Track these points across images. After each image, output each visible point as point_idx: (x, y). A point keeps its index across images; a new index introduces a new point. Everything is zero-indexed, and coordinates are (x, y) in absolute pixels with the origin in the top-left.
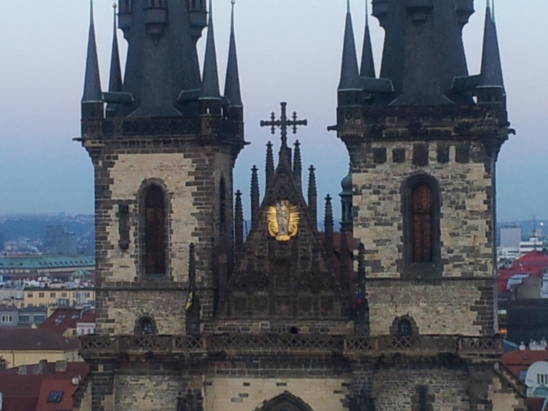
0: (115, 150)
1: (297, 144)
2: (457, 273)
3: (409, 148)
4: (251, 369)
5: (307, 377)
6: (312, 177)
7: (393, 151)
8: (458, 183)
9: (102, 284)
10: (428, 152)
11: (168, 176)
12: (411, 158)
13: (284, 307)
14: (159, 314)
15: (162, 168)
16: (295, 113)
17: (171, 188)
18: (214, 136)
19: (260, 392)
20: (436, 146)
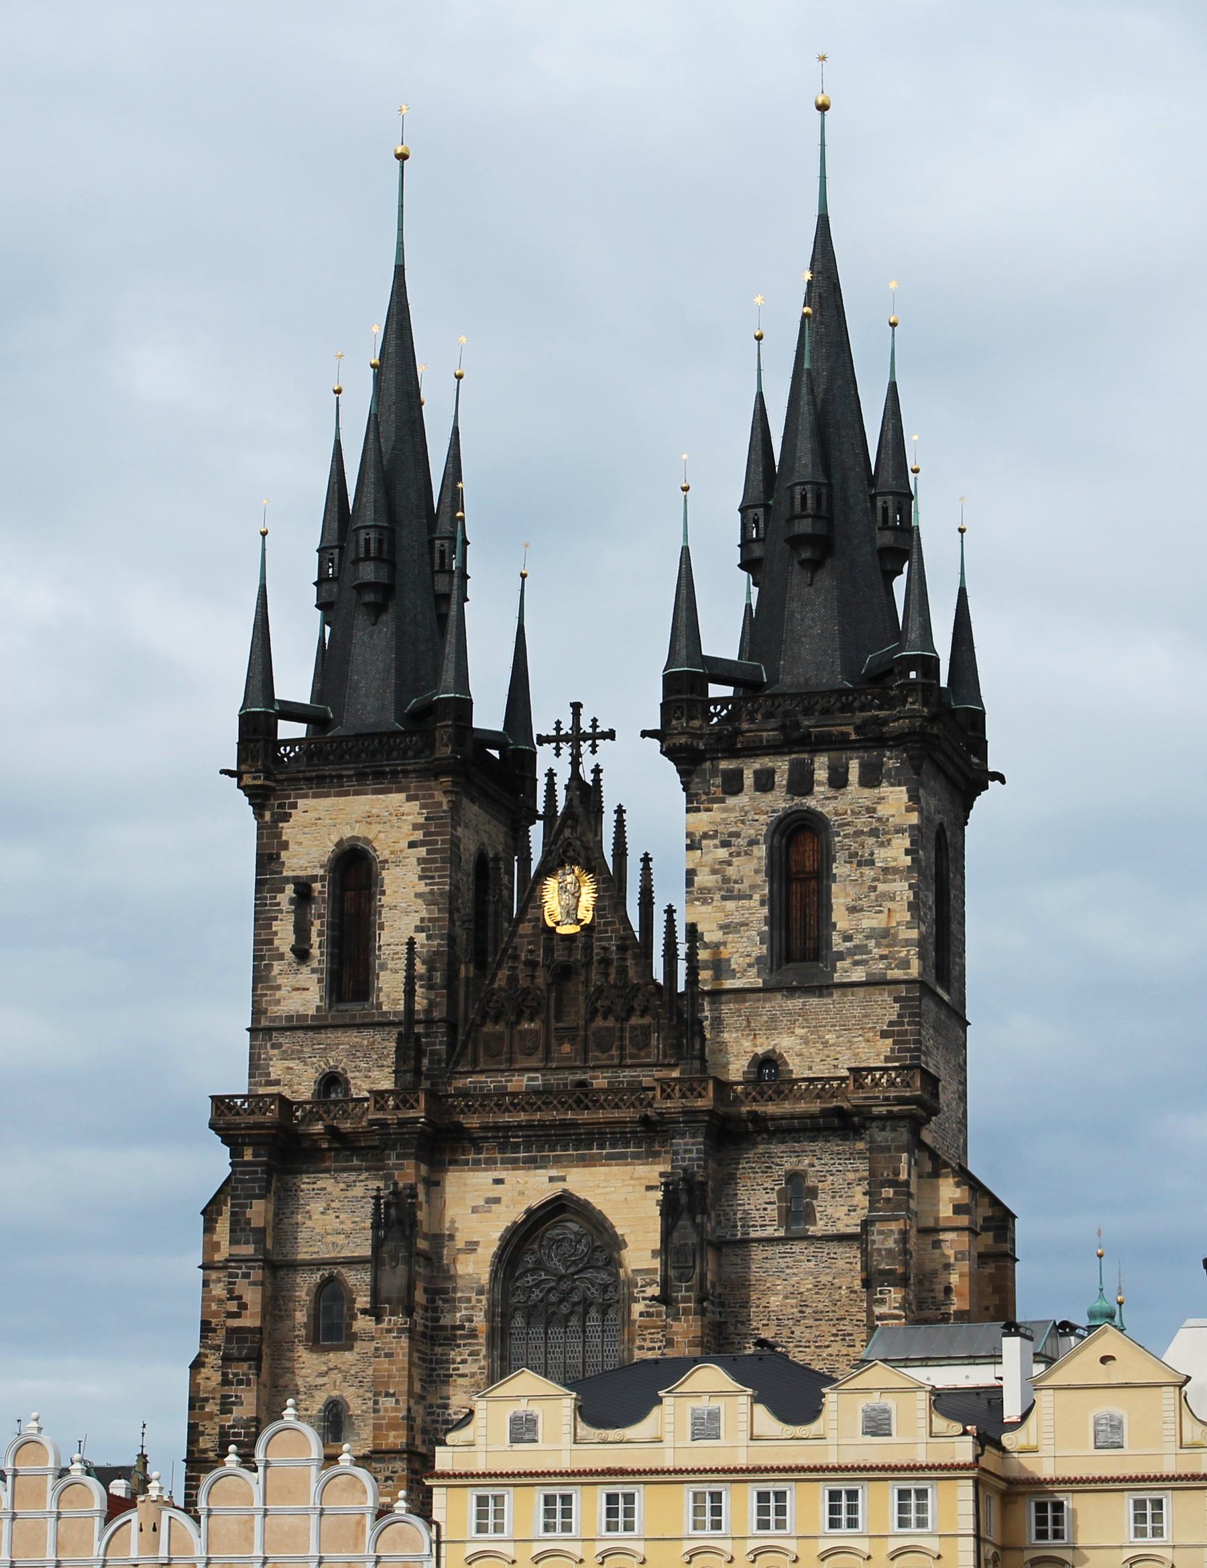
0: (293, 793)
1: (597, 771)
2: (858, 975)
3: (782, 766)
6: (620, 824)
7: (755, 772)
8: (862, 822)
12: (784, 782)
16: (595, 720)
17: (383, 853)
19: (522, 1193)
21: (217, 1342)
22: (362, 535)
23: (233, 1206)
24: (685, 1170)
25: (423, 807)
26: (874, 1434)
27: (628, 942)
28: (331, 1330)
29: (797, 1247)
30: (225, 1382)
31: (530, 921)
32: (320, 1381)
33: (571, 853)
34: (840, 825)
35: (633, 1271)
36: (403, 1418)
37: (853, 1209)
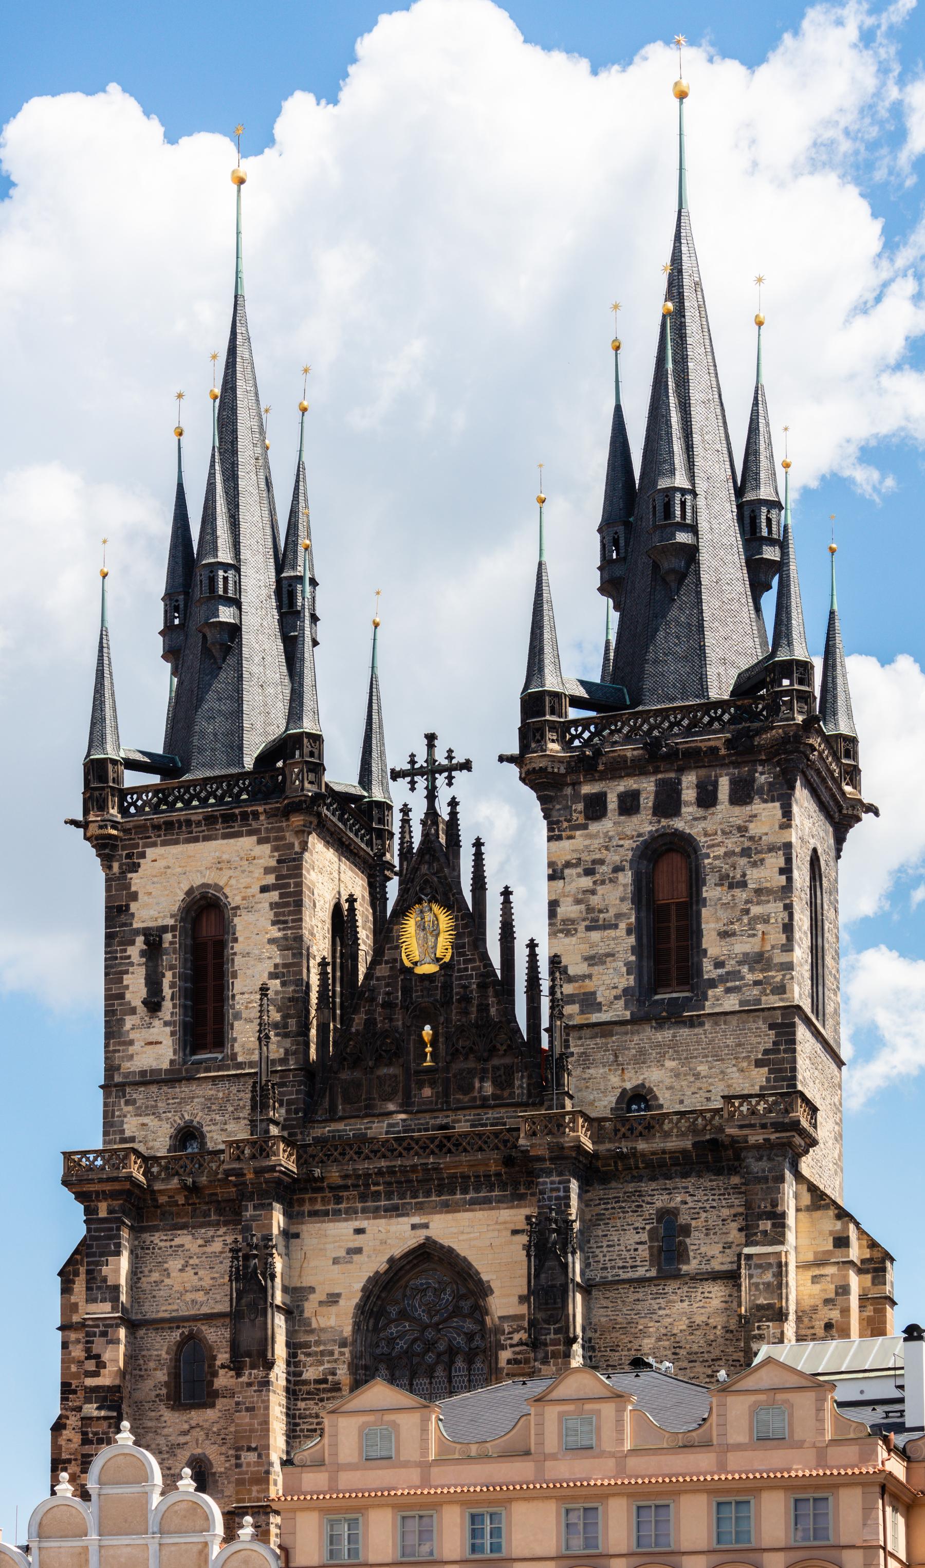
1: (453, 803)
2: (731, 1003)
3: (647, 787)
6: (479, 858)
10: (679, 793)
12: (650, 804)
13: (427, 1092)
16: (450, 751)
17: (235, 900)
19: (384, 1242)
23: (89, 1264)
25: (275, 849)
30: (86, 1441)
31: (387, 962)
32: (182, 1439)
34: (709, 847)
35: (500, 1318)
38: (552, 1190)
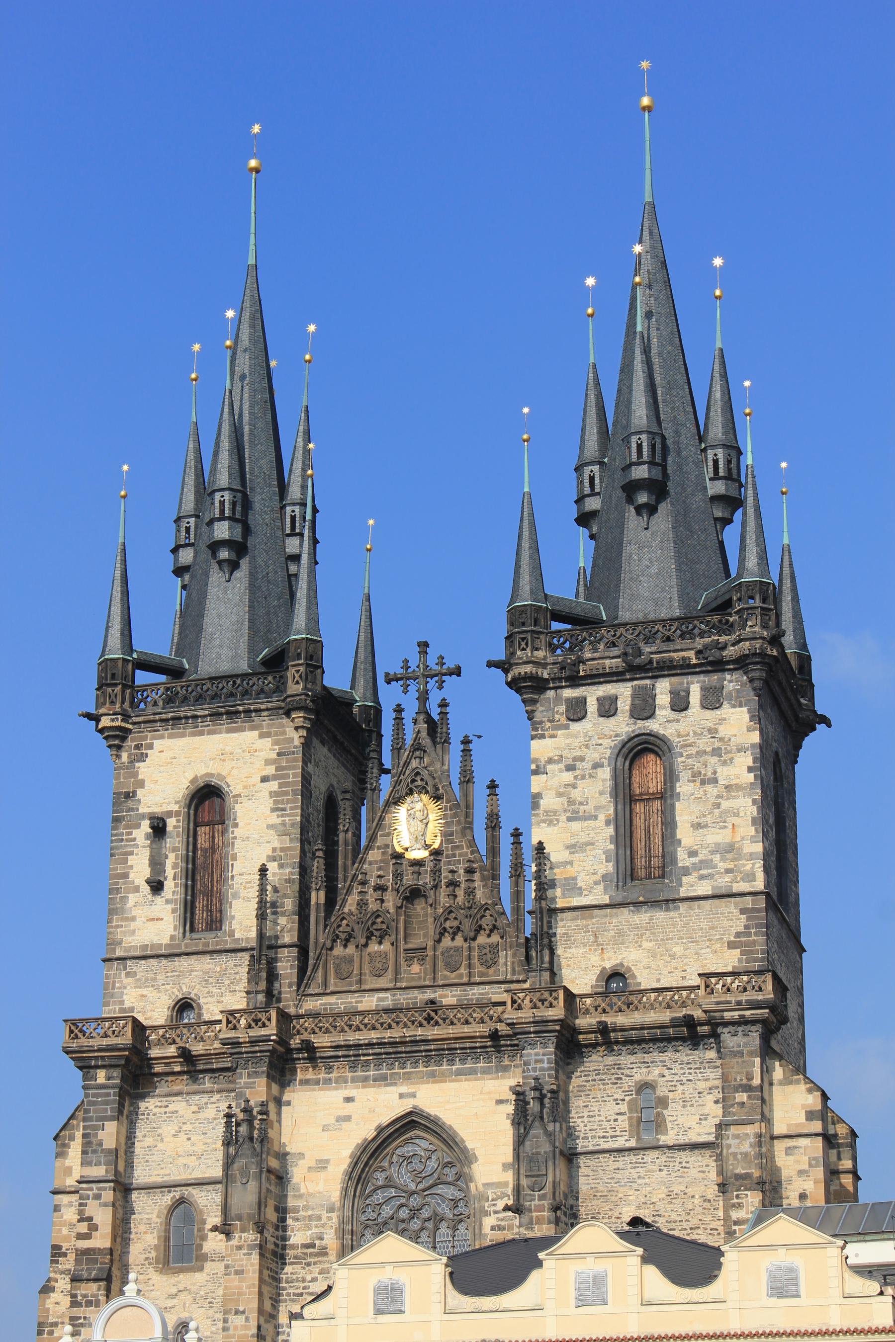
0: (149, 734)
1: (444, 704)
2: (704, 888)
3: (624, 692)
4: (359, 1073)
5: (453, 1081)
6: (466, 752)
8: (705, 743)
9: (118, 950)
11: (233, 768)
12: (628, 708)
13: (416, 968)
14: (208, 993)
15: (222, 757)
18: (307, 695)
20: (668, 684)
21: (68, 1267)
22: (217, 496)
23: (84, 1128)
24: (536, 1079)
25: (275, 743)
26: (780, 1296)
27: (475, 866)
28: (180, 1251)
29: (650, 1156)
30: (74, 1304)
31: (379, 848)
32: (170, 1303)
33: (419, 783)
34: (683, 747)
35: (484, 1185)
36: (252, 1336)
37: (703, 1118)
38: (537, 1061)
